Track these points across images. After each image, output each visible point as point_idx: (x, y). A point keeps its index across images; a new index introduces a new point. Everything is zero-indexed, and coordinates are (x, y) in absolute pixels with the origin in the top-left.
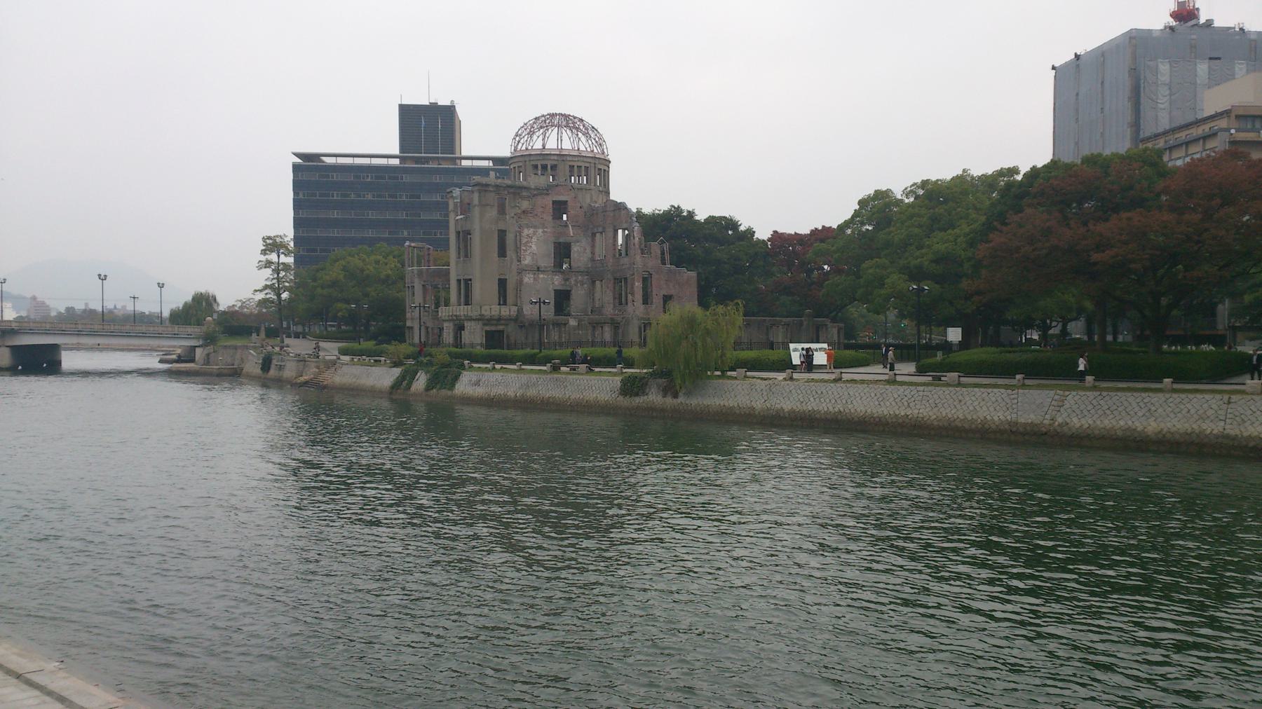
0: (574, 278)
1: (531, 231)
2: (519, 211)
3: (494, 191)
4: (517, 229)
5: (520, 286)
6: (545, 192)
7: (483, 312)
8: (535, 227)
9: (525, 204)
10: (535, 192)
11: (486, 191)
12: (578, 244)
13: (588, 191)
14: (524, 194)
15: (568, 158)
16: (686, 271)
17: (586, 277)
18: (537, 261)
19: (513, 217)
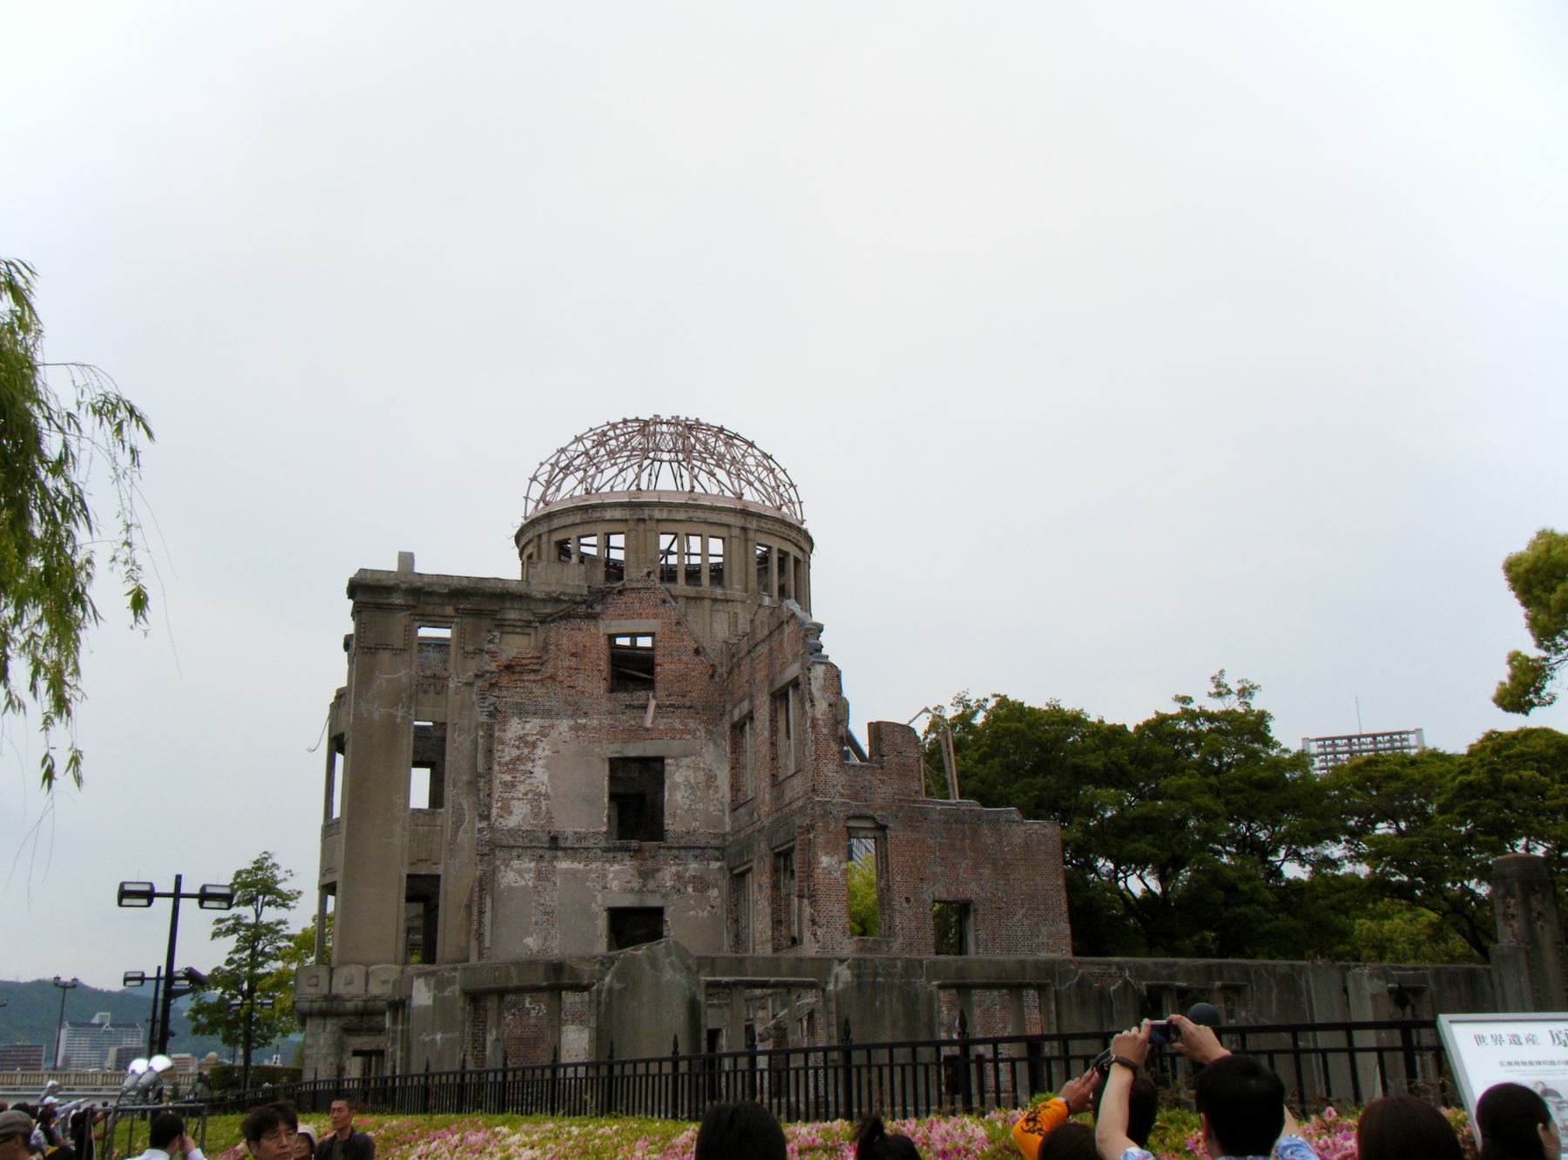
0: (674, 869)
1: (533, 725)
2: (493, 667)
3: (408, 607)
4: (483, 718)
5: (481, 898)
6: (582, 609)
7: (339, 988)
8: (547, 713)
9: (514, 646)
10: (548, 610)
11: (379, 607)
12: (685, 761)
13: (719, 606)
14: (513, 615)
15: (657, 514)
16: (1016, 816)
17: (715, 865)
18: (550, 818)
19: (471, 684)
